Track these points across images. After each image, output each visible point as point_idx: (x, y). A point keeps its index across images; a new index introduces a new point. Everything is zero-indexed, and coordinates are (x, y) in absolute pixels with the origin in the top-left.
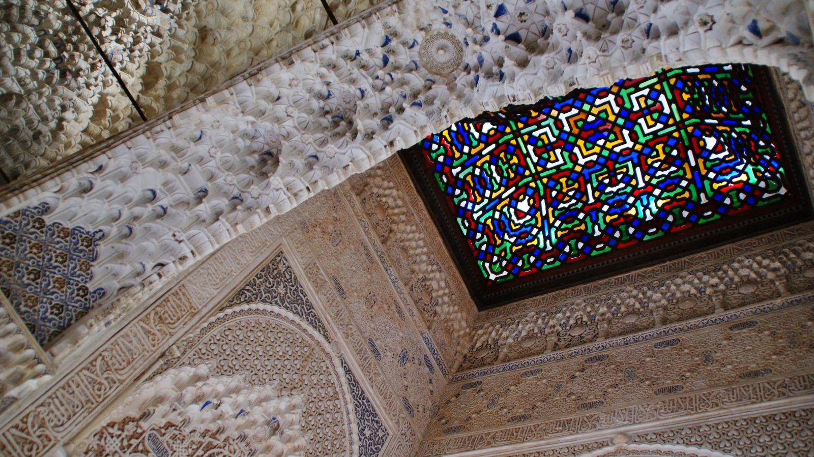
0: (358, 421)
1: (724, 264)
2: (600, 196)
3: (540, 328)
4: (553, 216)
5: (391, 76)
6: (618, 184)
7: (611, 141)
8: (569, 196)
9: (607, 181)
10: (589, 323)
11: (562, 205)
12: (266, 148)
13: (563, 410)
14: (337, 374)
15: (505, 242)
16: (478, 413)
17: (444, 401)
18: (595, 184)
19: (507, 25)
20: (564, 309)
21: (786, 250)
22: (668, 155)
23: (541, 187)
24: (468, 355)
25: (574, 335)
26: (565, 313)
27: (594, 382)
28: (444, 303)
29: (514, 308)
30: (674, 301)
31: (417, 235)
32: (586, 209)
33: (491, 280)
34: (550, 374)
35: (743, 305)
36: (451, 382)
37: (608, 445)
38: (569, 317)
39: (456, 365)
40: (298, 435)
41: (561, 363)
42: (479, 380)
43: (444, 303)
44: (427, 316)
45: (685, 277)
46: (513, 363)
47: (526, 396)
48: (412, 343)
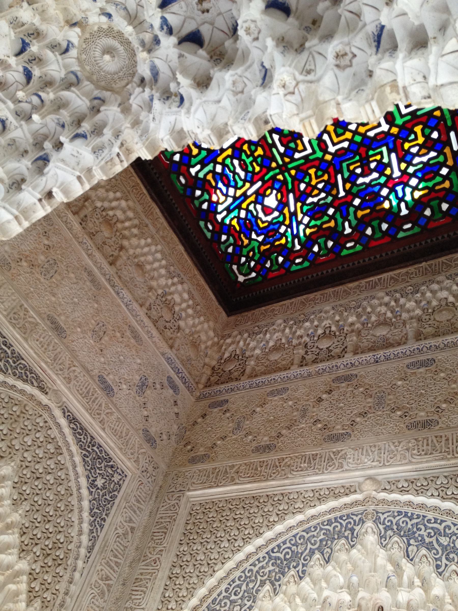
0: (87, 473)
2: (351, 188)
3: (287, 337)
4: (302, 212)
5: (40, 97)
6: (370, 174)
8: (318, 189)
10: (337, 333)
11: (310, 200)
13: (309, 442)
14: (58, 425)
15: (252, 242)
16: (223, 438)
18: (346, 174)
19: (183, 18)
20: (312, 317)
22: (427, 138)
23: (289, 179)
24: (217, 367)
25: (321, 347)
26: (312, 322)
27: (341, 408)
29: (262, 313)
30: (430, 311)
31: (153, 248)
32: (337, 203)
33: (239, 282)
34: (296, 394)
36: (199, 399)
37: (356, 491)
38: (317, 326)
40: (9, 511)
41: (308, 382)
42: (226, 398)
44: (169, 334)
45: (443, 282)
47: (271, 421)
48: (152, 367)
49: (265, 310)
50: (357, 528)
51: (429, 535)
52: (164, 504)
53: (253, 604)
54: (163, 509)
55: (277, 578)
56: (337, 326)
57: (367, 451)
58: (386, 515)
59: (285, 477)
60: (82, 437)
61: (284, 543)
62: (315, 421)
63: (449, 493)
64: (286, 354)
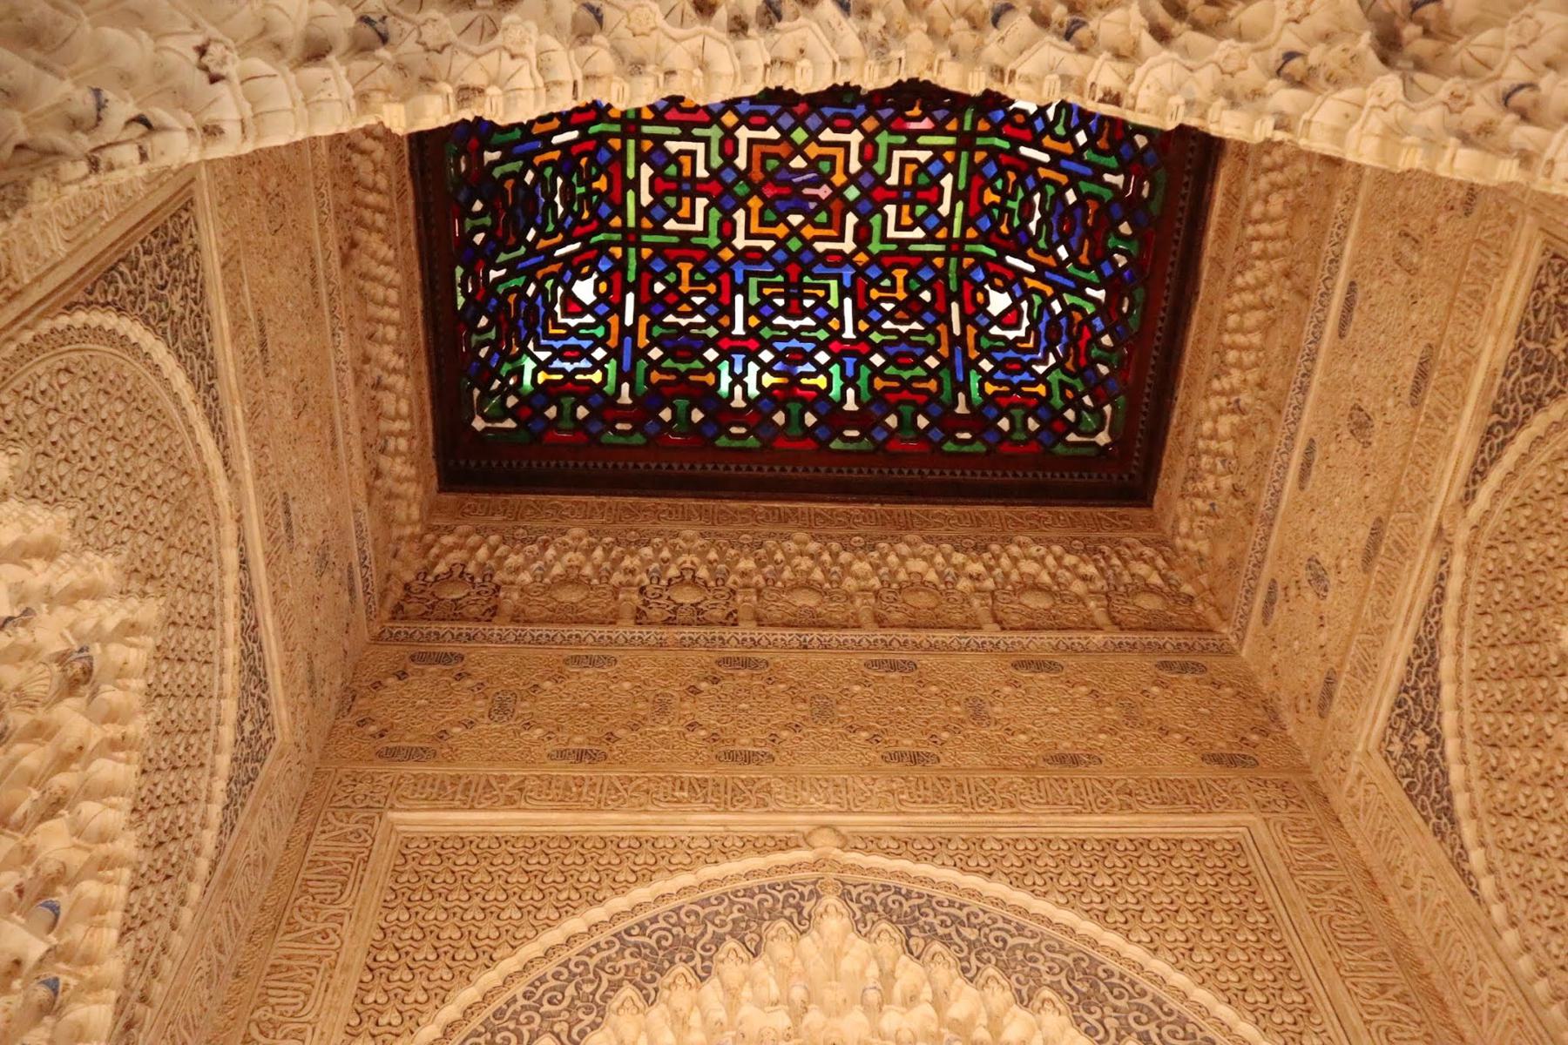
2: (759, 327)
3: (597, 568)
4: (649, 335)
6: (801, 317)
7: (816, 226)
8: (692, 304)
9: (780, 302)
11: (670, 318)
18: (754, 300)
20: (657, 540)
21: (1105, 548)
22: (913, 296)
23: (632, 264)
24: (415, 587)
25: (680, 601)
26: (658, 551)
28: (397, 453)
29: (529, 506)
33: (474, 430)
34: (637, 672)
36: (378, 639)
37: (798, 846)
38: (665, 561)
39: (390, 602)
41: (659, 654)
43: (397, 453)
46: (544, 630)
50: (808, 906)
51: (943, 923)
53: (599, 1020)
54: (324, 836)
55: (648, 977)
58: (860, 889)
61: (654, 920)
63: (972, 863)
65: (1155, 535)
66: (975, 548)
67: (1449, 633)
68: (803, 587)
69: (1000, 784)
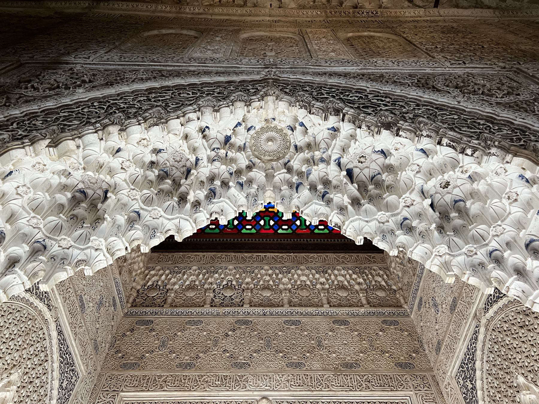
1: (329, 268)
10: (237, 287)
12: (81, 186)
17: (120, 332)
24: (141, 290)
25: (226, 295)
27: (242, 344)
30: (296, 287)
35: (340, 306)
36: (126, 315)
39: (131, 300)
41: (217, 320)
45: (304, 270)
46: (180, 310)
47: (190, 344)
49: (182, 255)
52: (100, 401)
56: (237, 282)
57: (262, 378)
59: (205, 390)
60: (62, 346)
62: (224, 351)
64: (199, 294)
65: (384, 265)
66: (323, 272)
67: (479, 353)
68: (266, 288)
69: (325, 377)
